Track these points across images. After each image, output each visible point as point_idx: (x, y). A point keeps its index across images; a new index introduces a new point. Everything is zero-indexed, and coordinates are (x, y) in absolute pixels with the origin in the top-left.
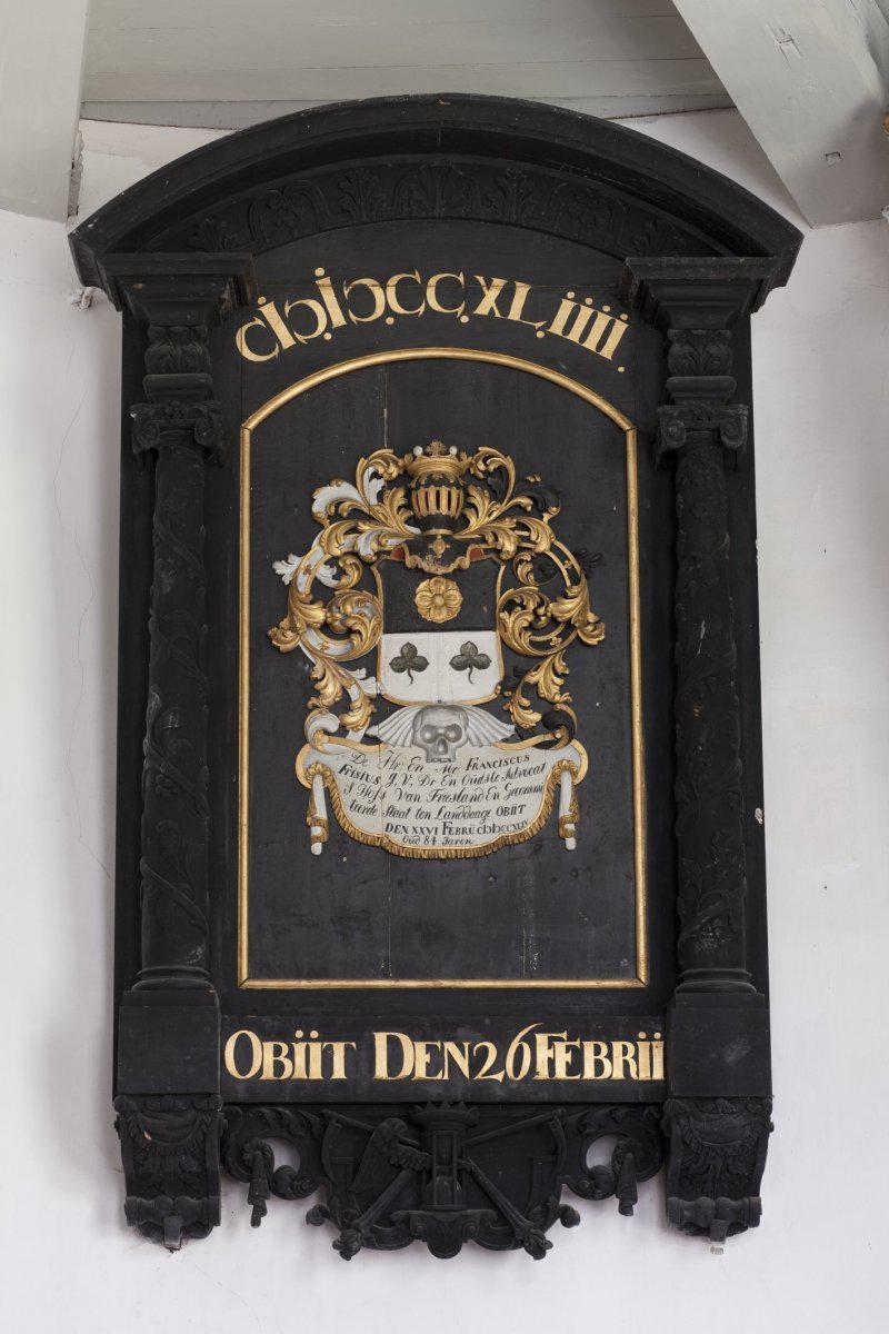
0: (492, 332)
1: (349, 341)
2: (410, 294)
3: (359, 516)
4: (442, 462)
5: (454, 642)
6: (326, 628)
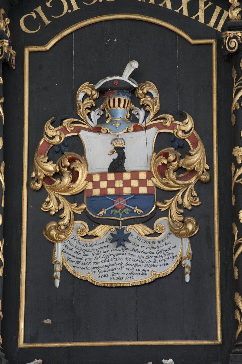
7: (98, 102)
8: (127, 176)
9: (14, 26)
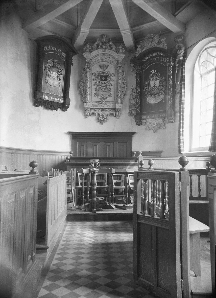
0: (58, 53)
1: (51, 51)
2: (54, 49)
3: (50, 63)
4: (55, 61)
5: (55, 73)
6: (48, 70)
7: (152, 77)
8: (156, 87)
9: (142, 68)
